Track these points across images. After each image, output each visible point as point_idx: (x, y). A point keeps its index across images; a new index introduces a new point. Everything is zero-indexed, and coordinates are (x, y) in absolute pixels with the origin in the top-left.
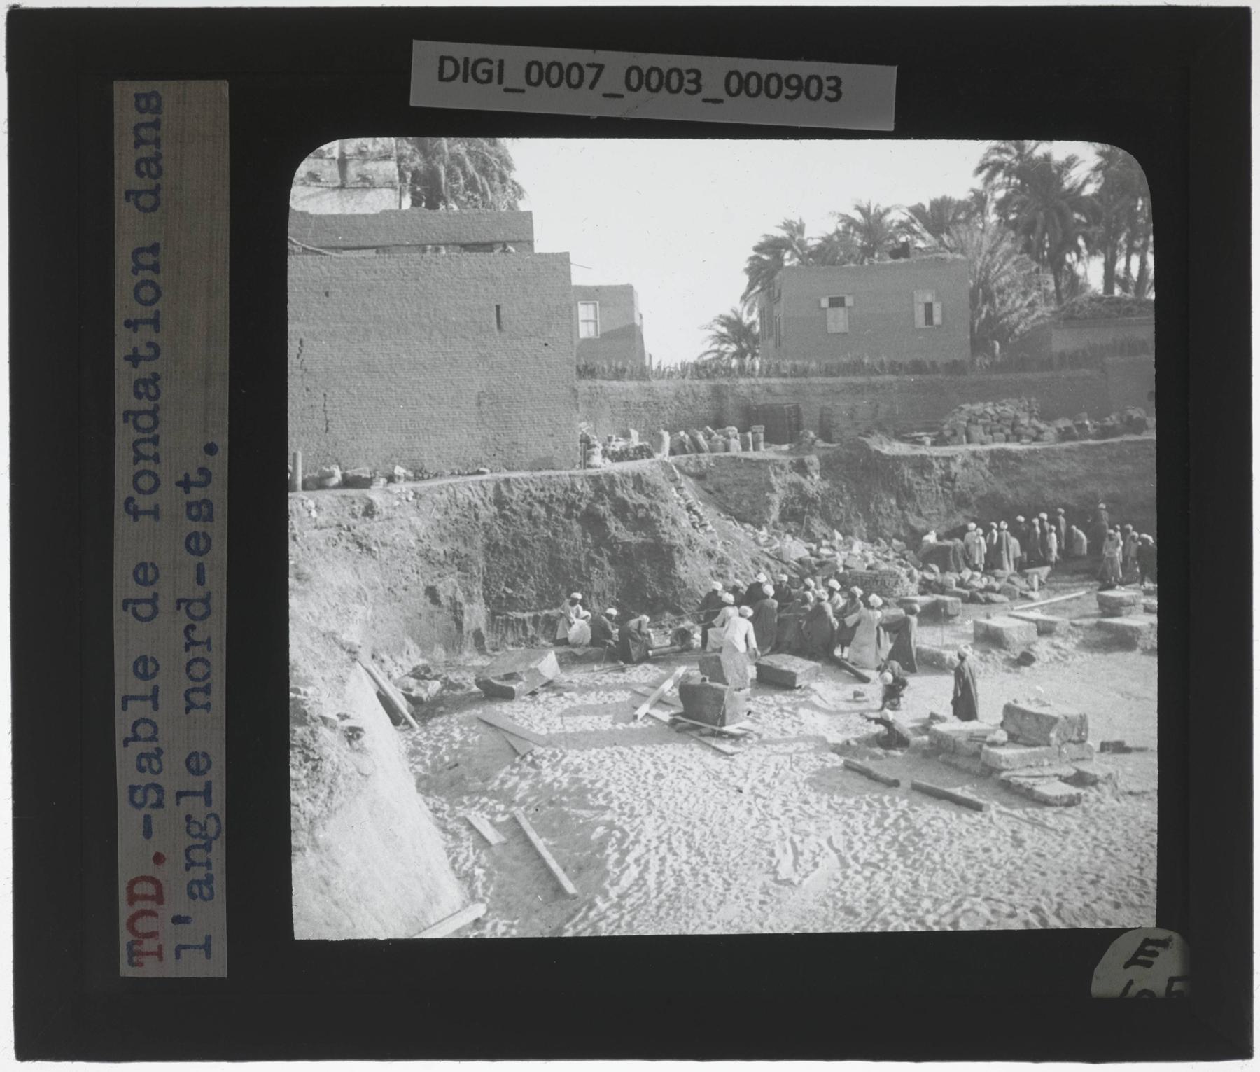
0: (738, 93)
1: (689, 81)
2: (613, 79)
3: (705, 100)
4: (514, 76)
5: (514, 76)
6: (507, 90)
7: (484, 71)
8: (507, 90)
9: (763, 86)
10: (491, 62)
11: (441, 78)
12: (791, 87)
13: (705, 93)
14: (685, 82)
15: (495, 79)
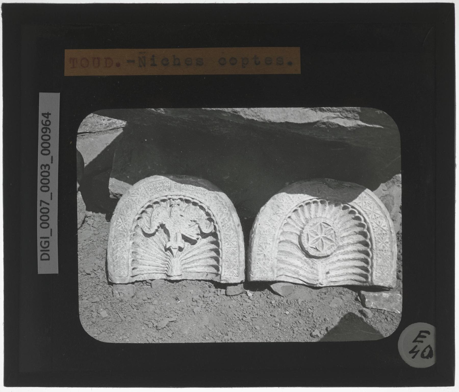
0: (49, 151)
1: (45, 168)
3: (52, 163)
6: (51, 235)
7: (45, 244)
8: (51, 235)
9: (45, 141)
10: (42, 241)
11: (49, 259)
12: (46, 132)
13: (49, 163)
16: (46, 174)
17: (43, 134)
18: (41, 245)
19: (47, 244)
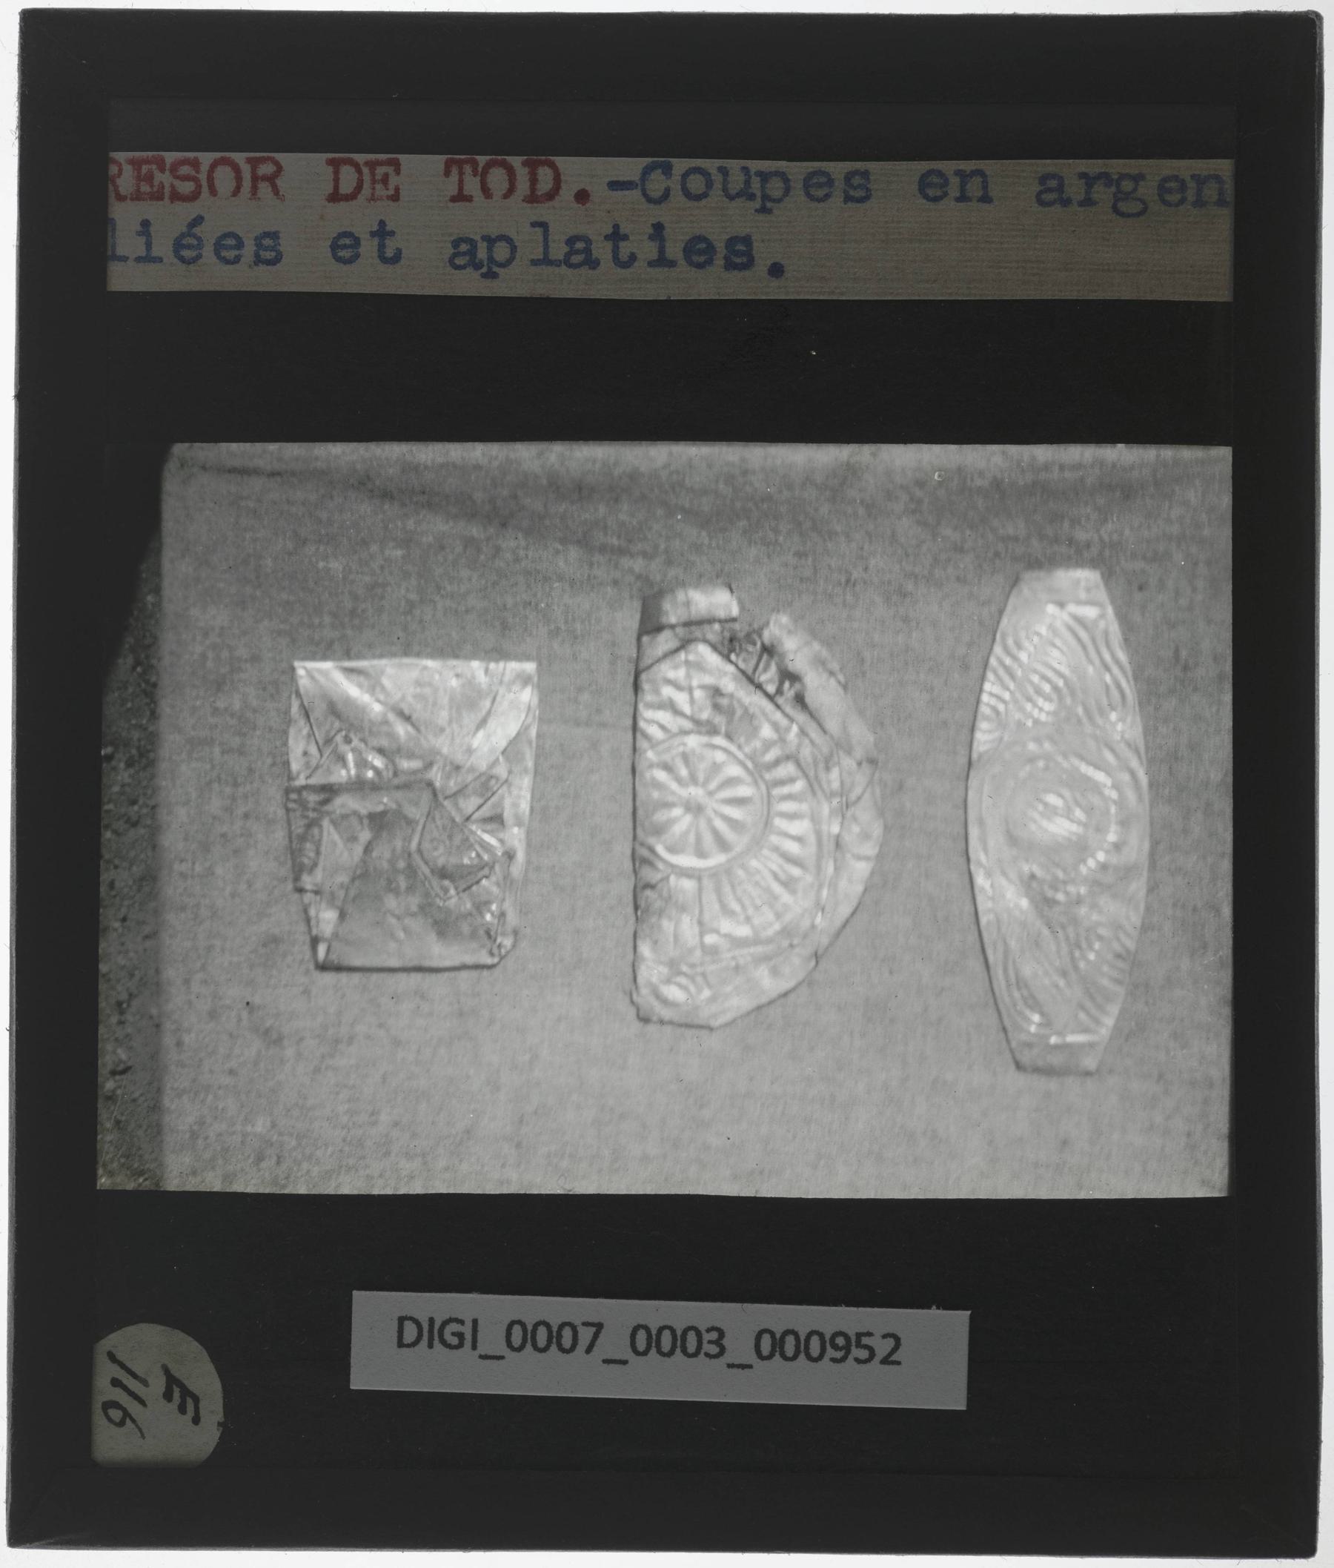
1: (710, 1342)
2: (613, 1343)
3: (730, 1366)
4: (492, 1340)
5: (492, 1340)
6: (481, 1357)
7: (453, 1334)
8: (481, 1357)
9: (803, 1348)
10: (462, 1322)
13: (728, 1358)
14: (705, 1342)
15: (468, 1337)
16: (691, 1348)
17: (828, 1337)
18: (451, 1320)
19: (455, 1341)
